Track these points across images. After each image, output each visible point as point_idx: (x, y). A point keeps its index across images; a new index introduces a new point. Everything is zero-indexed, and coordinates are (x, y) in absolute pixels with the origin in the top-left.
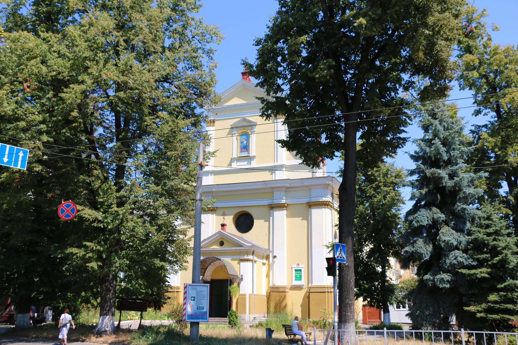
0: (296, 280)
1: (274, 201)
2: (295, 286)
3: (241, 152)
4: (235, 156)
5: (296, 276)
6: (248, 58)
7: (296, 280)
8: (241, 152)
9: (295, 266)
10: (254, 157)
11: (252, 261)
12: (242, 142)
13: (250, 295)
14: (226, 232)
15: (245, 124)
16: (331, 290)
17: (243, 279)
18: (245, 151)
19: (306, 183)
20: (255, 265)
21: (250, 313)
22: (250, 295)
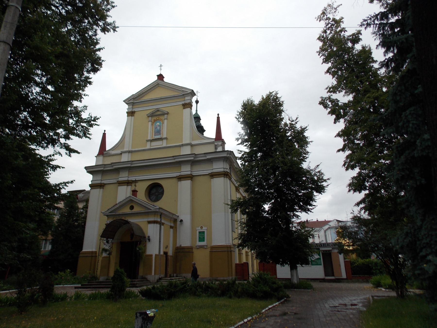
0: (199, 241)
1: (182, 173)
2: (199, 246)
3: (155, 135)
4: (149, 138)
5: (199, 238)
6: (162, 65)
7: (199, 241)
8: (155, 135)
9: (199, 228)
10: (166, 138)
11: (160, 223)
12: (156, 128)
13: (156, 255)
14: (137, 197)
15: (159, 113)
16: (230, 249)
17: (151, 240)
18: (158, 135)
19: (209, 157)
20: (162, 227)
21: (155, 274)
22: (156, 255)
